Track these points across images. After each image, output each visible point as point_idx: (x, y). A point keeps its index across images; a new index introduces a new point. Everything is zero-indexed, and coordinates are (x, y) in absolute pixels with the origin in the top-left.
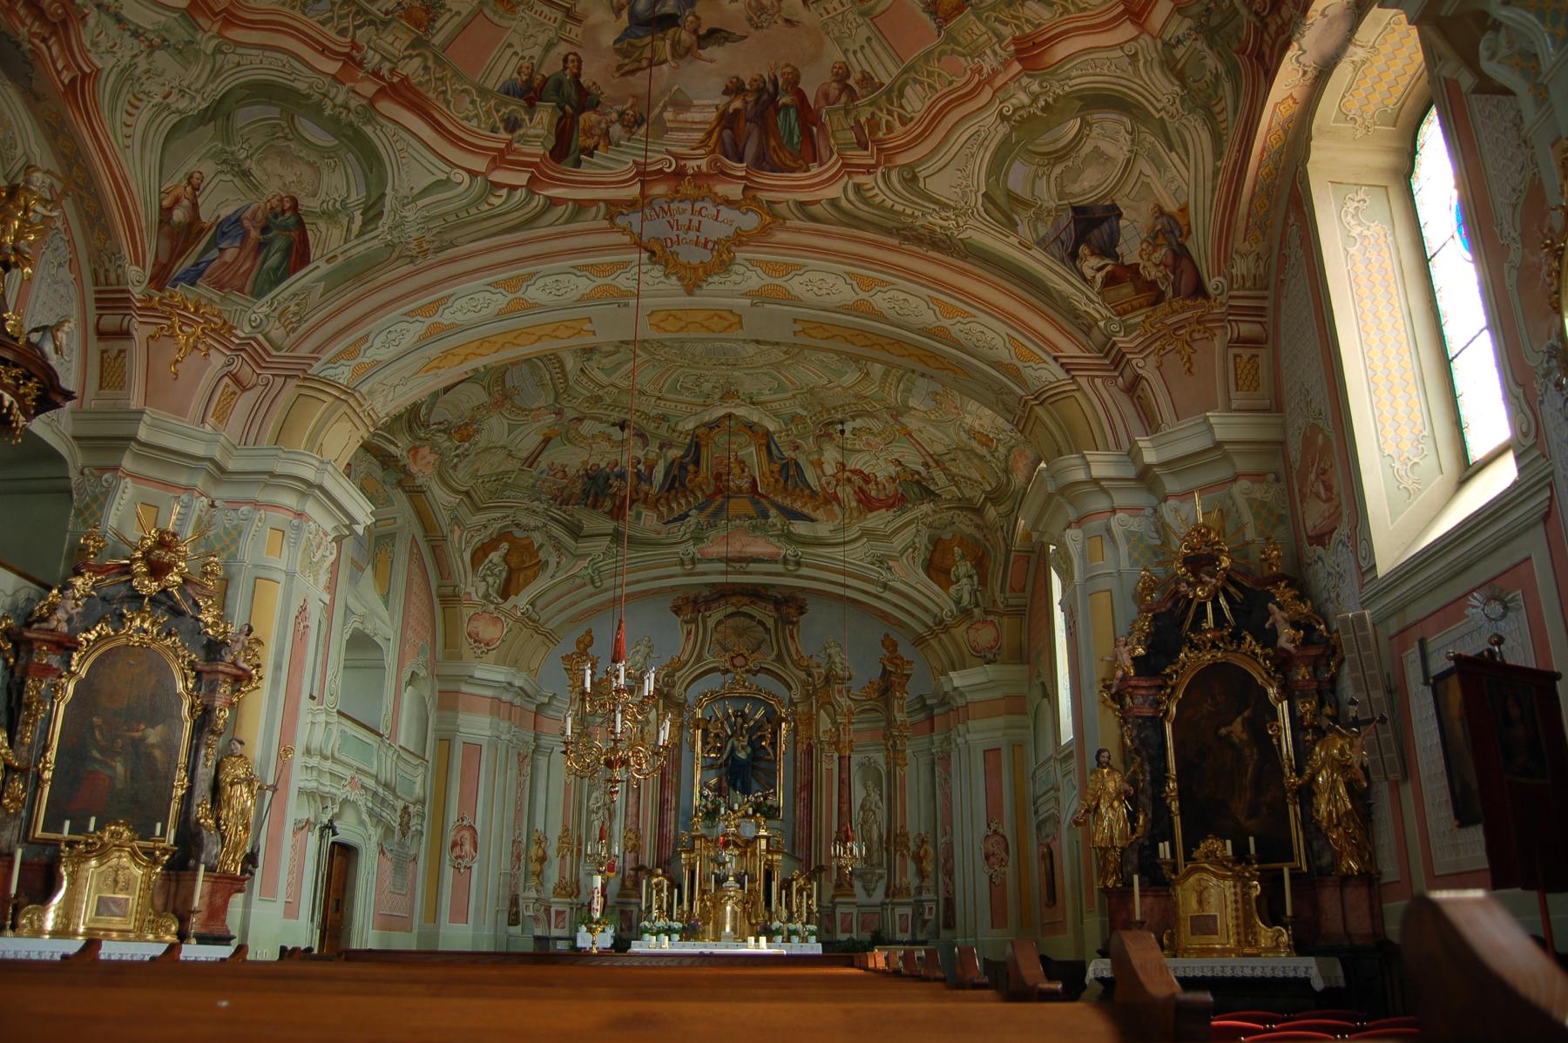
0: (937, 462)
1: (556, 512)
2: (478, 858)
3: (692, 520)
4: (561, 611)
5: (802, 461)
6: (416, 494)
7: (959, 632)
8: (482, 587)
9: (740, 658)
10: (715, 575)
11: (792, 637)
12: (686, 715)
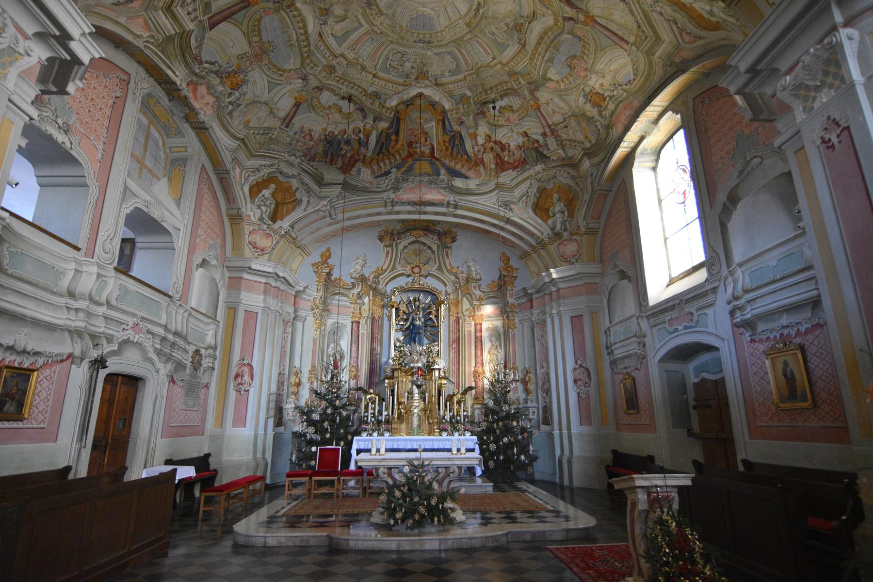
0: (552, 131)
1: (306, 166)
2: (253, 384)
3: (393, 176)
4: (311, 234)
5: (464, 133)
6: (201, 129)
7: (552, 248)
8: (258, 212)
9: (417, 268)
10: (406, 214)
11: (447, 256)
12: (386, 300)
